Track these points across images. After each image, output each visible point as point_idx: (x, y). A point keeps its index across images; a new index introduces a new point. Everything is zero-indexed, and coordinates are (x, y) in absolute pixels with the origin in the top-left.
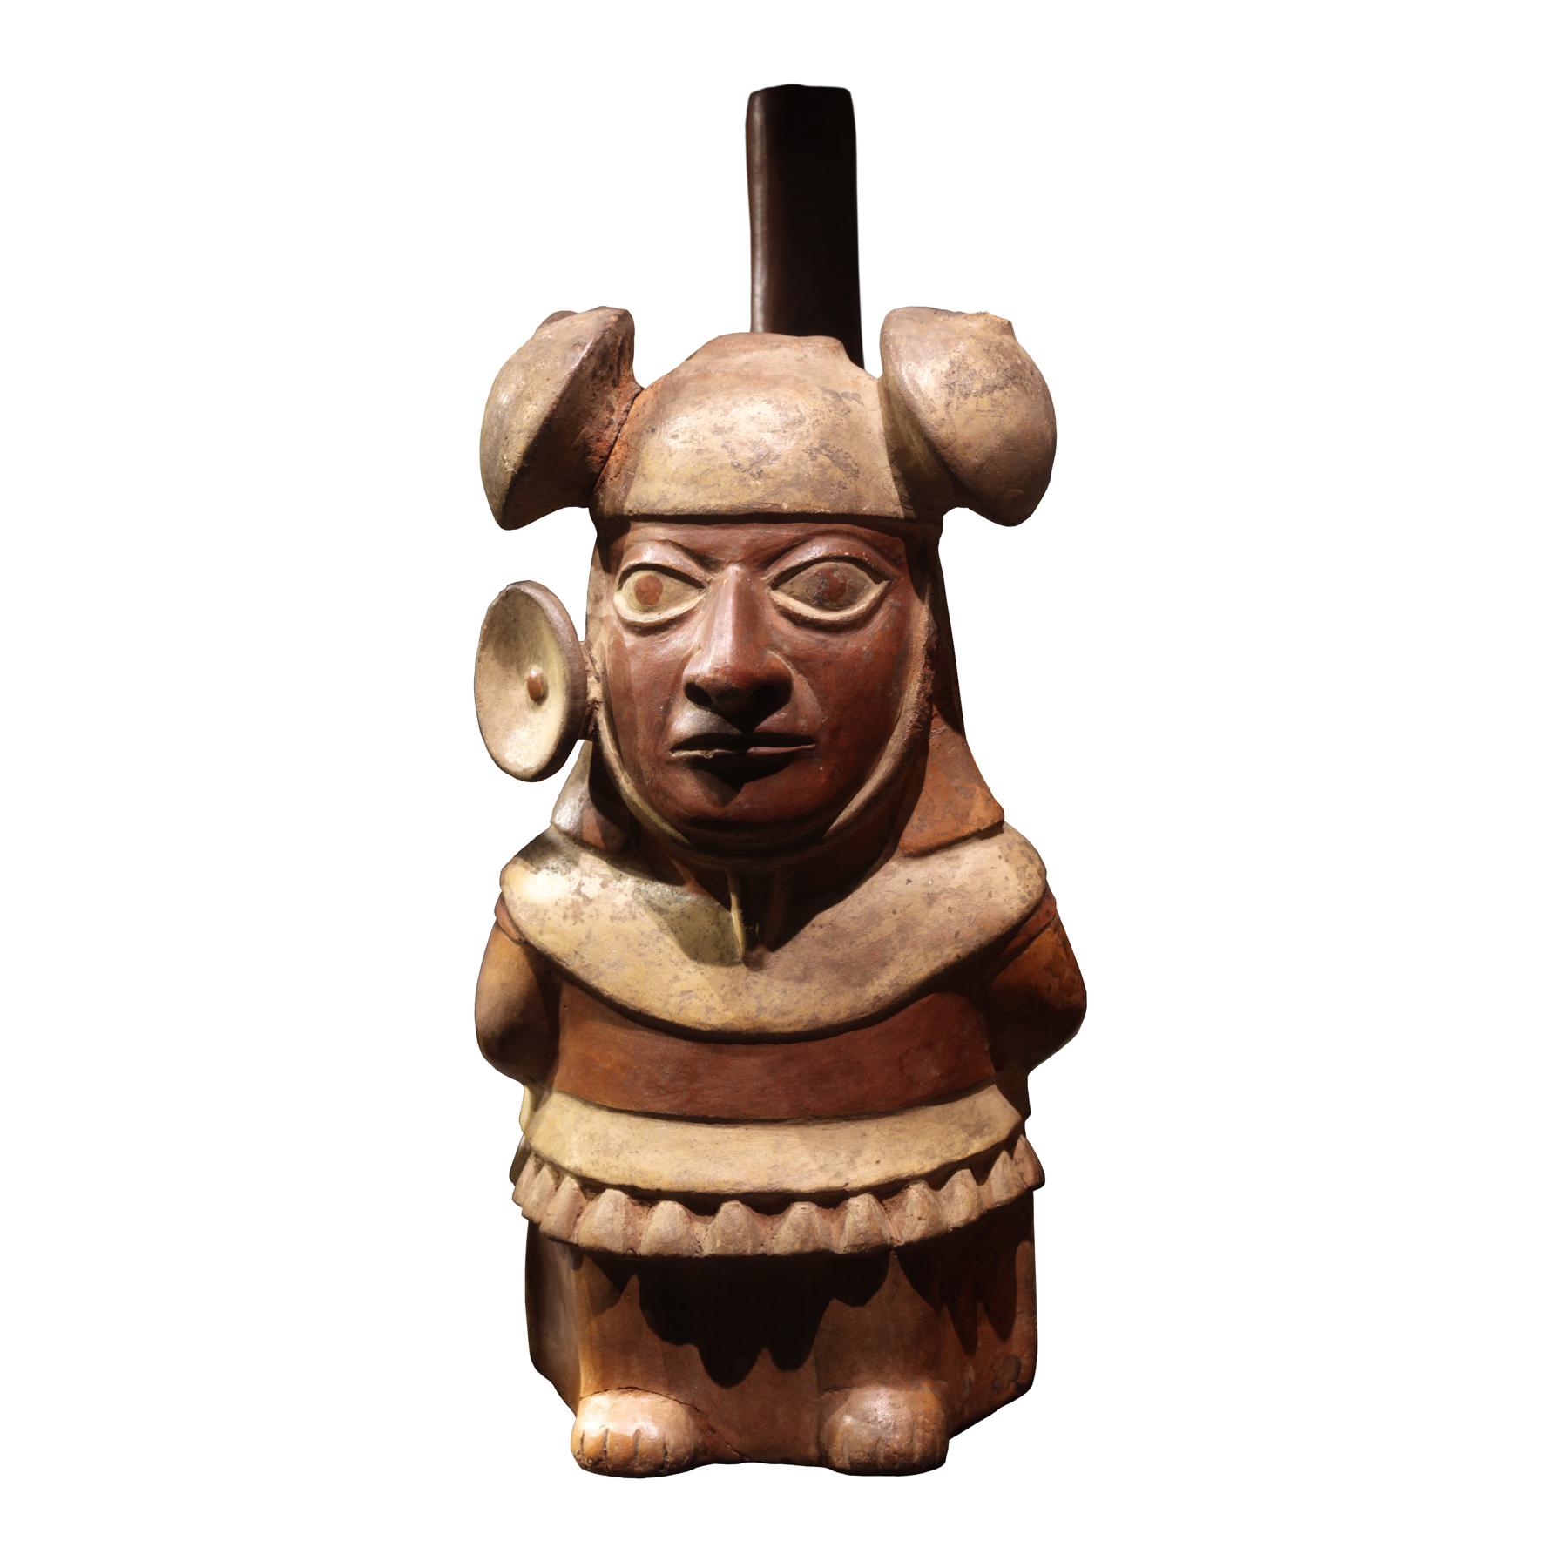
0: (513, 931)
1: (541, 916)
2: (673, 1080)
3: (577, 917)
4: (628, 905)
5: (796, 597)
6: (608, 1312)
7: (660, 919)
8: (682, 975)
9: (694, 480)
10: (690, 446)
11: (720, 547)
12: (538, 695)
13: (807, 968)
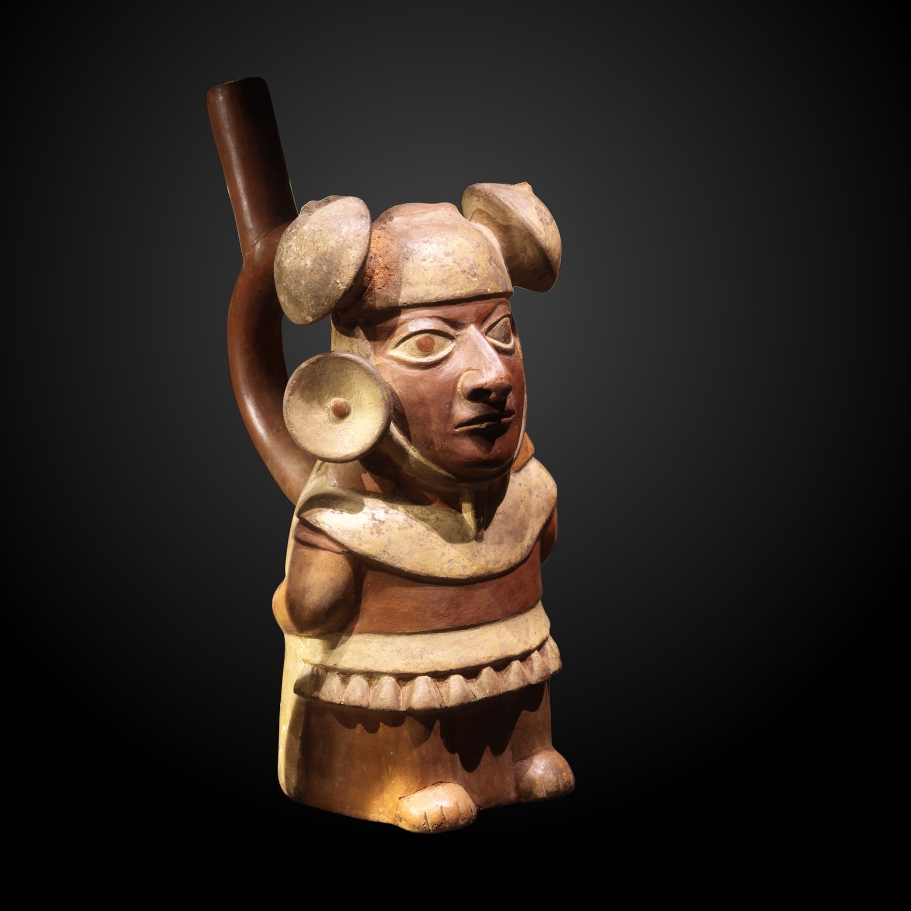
0: (336, 548)
1: (357, 535)
2: (447, 609)
3: (379, 532)
4: (405, 520)
5: (495, 339)
6: (424, 744)
7: (426, 524)
8: (446, 552)
9: (444, 282)
10: (436, 264)
11: (464, 316)
12: (341, 413)
13: (500, 537)
